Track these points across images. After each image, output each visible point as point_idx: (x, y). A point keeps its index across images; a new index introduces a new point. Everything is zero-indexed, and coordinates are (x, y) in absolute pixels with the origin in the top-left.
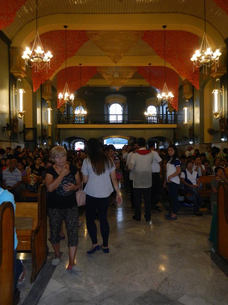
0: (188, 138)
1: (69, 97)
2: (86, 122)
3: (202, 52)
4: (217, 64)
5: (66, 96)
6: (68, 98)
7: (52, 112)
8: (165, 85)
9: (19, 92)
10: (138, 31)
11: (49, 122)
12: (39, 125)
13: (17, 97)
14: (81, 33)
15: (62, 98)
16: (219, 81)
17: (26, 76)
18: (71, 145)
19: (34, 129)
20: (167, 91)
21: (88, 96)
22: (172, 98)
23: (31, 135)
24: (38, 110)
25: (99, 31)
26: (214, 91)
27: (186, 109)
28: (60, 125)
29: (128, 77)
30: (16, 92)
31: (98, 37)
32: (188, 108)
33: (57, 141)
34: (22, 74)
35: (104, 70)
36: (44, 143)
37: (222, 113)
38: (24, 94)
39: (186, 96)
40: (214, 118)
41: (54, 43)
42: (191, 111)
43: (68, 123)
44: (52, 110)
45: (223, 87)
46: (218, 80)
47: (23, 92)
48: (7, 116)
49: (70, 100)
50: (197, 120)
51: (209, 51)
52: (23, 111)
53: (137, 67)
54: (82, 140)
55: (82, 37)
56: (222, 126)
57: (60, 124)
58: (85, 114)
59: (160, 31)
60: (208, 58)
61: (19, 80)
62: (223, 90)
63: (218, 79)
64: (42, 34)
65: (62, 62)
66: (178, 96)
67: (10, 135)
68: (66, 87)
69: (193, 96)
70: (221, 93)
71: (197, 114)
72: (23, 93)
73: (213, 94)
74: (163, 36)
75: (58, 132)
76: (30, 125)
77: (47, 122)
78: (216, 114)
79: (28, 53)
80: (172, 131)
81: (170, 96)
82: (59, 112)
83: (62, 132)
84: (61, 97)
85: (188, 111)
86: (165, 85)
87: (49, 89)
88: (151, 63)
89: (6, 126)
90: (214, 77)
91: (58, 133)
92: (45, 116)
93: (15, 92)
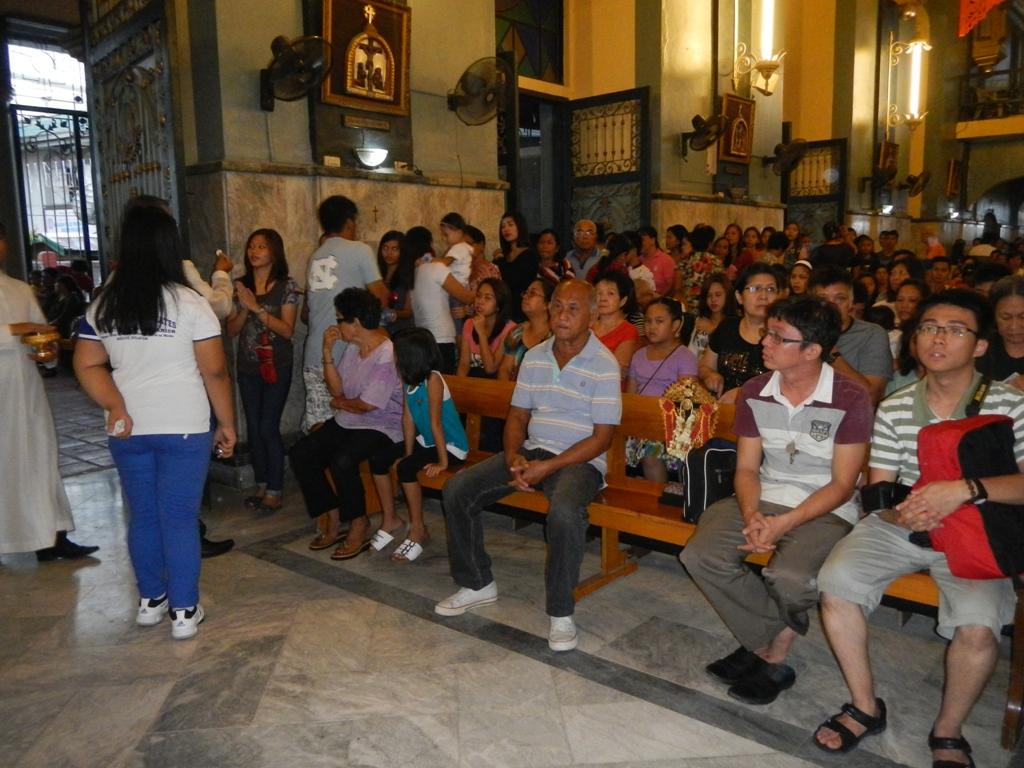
7: (934, 61)
11: (915, 108)
12: (862, 129)
19: (839, 147)
24: (863, 62)
28: (971, 123)
33: (950, 200)
36: (881, 207)
44: (928, 48)
48: (703, 89)
52: (774, 53)
67: (712, 169)
75: (960, 158)
76: (816, 127)
77: (905, 108)
82: (972, 63)
83: (978, 156)
89: (691, 129)
91: (956, 163)
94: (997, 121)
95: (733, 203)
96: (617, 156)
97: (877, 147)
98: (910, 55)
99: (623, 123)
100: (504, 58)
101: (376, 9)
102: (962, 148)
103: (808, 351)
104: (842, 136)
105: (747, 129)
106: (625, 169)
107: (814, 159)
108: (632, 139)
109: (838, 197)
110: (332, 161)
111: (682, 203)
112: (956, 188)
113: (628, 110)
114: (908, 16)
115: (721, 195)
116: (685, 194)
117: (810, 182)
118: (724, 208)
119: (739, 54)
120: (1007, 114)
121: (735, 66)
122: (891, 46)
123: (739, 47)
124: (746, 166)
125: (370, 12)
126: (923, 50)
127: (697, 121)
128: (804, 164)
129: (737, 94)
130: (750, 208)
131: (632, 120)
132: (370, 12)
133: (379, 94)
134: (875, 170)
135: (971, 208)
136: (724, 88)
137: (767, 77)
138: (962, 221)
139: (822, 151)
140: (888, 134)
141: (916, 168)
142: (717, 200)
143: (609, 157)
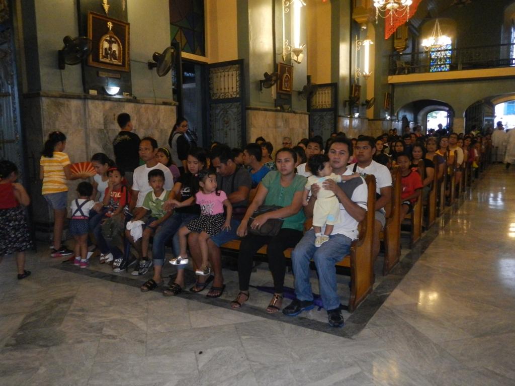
2: (453, 68)
13: (289, 16)
18: (420, 118)
19: (334, 86)
21: (461, 6)
23: (327, 98)
24: (344, 48)
28: (394, 76)
30: (287, 7)
33: (386, 111)
36: (354, 114)
43: (412, 71)
44: (372, 43)
47: (303, 4)
48: (269, 60)
52: (300, 45)
54: (442, 107)
57: (395, 75)
75: (390, 91)
77: (363, 70)
82: (394, 49)
83: (398, 91)
84: (379, 2)
89: (263, 78)
91: (388, 94)
93: (285, 8)
94: (404, 76)
95: (284, 112)
96: (230, 90)
97: (351, 87)
98: (364, 46)
99: (232, 75)
100: (174, 44)
101: (113, 23)
102: (390, 87)
103: (228, 163)
105: (290, 79)
106: (234, 96)
107: (323, 92)
108: (237, 82)
110: (93, 92)
111: (260, 112)
113: (234, 69)
114: (363, 29)
115: (279, 108)
116: (262, 107)
117: (322, 102)
118: (280, 114)
119: (285, 45)
120: (409, 73)
121: (284, 50)
122: (357, 42)
123: (285, 42)
124: (290, 96)
125: (110, 25)
126: (370, 44)
127: (266, 75)
129: (285, 63)
130: (293, 114)
131: (236, 74)
132: (110, 25)
133: (115, 62)
134: (350, 97)
135: (396, 115)
136: (279, 60)
137: (298, 56)
138: (391, 120)
139: (327, 88)
140: (356, 81)
142: (277, 111)
143: (227, 91)
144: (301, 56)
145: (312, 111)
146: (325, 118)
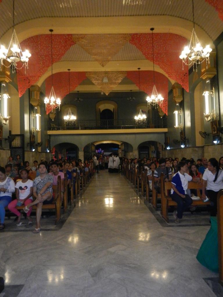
0: (179, 142)
1: (55, 101)
3: (191, 49)
4: (208, 61)
5: (53, 100)
6: (55, 102)
8: (154, 88)
9: (4, 97)
10: (126, 34)
11: (38, 128)
12: (27, 132)
14: (67, 37)
15: (48, 102)
16: (209, 83)
17: (11, 81)
19: (22, 136)
20: (156, 93)
22: (162, 101)
24: (26, 116)
25: (86, 35)
26: (205, 93)
27: (176, 112)
29: (118, 81)
31: (85, 41)
32: (179, 112)
34: (6, 79)
35: (93, 76)
36: (32, 150)
37: (213, 115)
38: (9, 99)
39: (177, 100)
40: (205, 120)
41: (39, 47)
42: (182, 114)
43: (58, 129)
44: (40, 116)
45: (214, 89)
46: (208, 82)
47: (8, 97)
49: (56, 105)
50: (188, 124)
51: (198, 47)
52: (7, 116)
53: (126, 72)
55: (69, 40)
56: (214, 128)
58: (74, 120)
59: (148, 34)
60: (198, 55)
61: (4, 86)
62: (214, 92)
63: (209, 81)
64: (28, 39)
65: (48, 67)
66: (167, 100)
68: (52, 92)
69: (183, 99)
70: (211, 94)
71: (188, 117)
72: (7, 99)
73: (204, 96)
74: (151, 39)
75: (49, 139)
76: (16, 131)
77: (36, 128)
78: (207, 117)
79: (4, 52)
80: (163, 135)
81: (160, 99)
83: (52, 138)
85: (179, 114)
86: (155, 87)
87: (37, 94)
88: (140, 67)
90: (204, 79)
91: (48, 140)
92: (33, 123)
102: (49, 136)
104: (22, 133)
109: (22, 147)
112: (48, 145)
120: (57, 130)
128: (16, 139)
130: (3, 150)
141: (39, 141)
144: (8, 121)
145: (11, 148)
146: (17, 152)
